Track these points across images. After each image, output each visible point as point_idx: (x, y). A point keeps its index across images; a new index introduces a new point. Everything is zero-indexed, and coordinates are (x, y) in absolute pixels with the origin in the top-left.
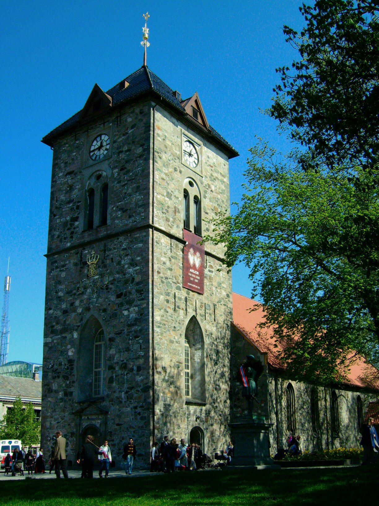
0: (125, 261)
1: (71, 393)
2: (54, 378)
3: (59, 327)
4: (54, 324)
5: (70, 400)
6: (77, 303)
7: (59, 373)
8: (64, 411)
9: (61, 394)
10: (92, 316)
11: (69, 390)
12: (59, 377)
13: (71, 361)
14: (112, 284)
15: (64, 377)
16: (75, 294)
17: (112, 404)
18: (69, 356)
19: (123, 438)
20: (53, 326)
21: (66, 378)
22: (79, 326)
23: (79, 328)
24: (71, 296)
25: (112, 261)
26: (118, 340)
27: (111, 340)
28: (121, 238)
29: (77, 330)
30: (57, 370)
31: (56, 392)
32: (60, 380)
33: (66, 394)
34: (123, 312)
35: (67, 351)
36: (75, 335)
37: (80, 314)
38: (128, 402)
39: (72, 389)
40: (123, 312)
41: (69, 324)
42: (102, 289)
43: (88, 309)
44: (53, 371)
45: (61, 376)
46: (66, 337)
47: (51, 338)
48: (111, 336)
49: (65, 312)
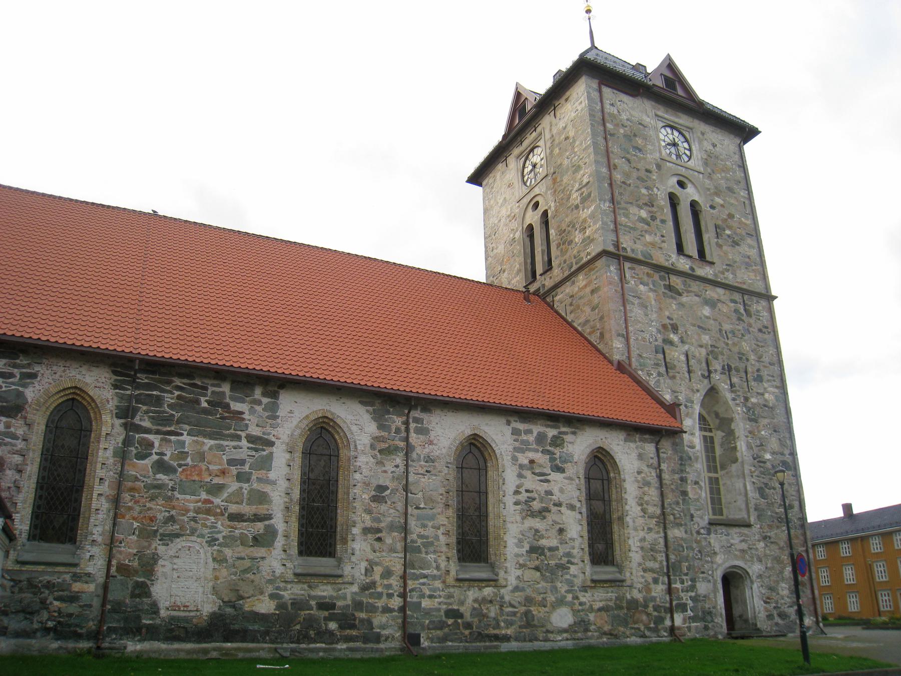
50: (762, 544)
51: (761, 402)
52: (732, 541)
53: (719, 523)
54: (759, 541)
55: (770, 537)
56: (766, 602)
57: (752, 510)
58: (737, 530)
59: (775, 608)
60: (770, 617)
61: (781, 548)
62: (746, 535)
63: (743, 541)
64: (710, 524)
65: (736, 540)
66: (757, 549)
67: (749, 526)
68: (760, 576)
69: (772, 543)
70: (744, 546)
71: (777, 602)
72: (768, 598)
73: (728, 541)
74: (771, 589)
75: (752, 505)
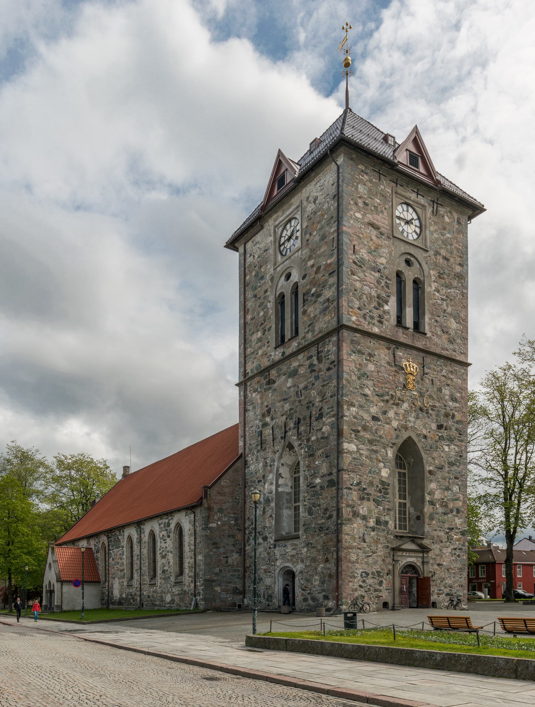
0: (446, 391)
1: (386, 523)
2: (362, 499)
3: (367, 436)
4: (360, 428)
5: (384, 530)
6: (391, 414)
7: (368, 494)
8: (377, 542)
9: (372, 523)
10: (410, 437)
11: (383, 518)
12: (369, 500)
13: (383, 483)
14: (432, 410)
15: (374, 500)
16: (387, 401)
17: (433, 543)
18: (382, 477)
19: (444, 579)
20: (359, 431)
21: (377, 503)
22: (394, 444)
23: (395, 447)
24: (383, 401)
25: (432, 384)
26: (439, 475)
27: (430, 472)
28: (440, 362)
29: (391, 447)
30: (364, 489)
31: (364, 518)
32: (372, 504)
33: (378, 522)
34: (444, 446)
35: (380, 471)
36: (390, 453)
37: (396, 430)
38: (448, 543)
39: (387, 518)
40: (444, 446)
41: (380, 437)
42: (421, 409)
43: (406, 428)
44: (359, 490)
45: (371, 499)
46: (376, 452)
47: (357, 446)
48: (431, 468)
49: (375, 418)
50: (305, 549)
51: (320, 436)
52: (287, 550)
53: (281, 539)
54: (304, 547)
55: (312, 544)
56: (303, 590)
57: (301, 526)
58: (290, 542)
59: (309, 593)
60: (305, 600)
61: (318, 551)
62: (296, 545)
63: (293, 549)
64: (275, 541)
65: (289, 549)
66: (302, 553)
67: (298, 537)
68: (301, 572)
69: (313, 547)
70: (294, 553)
71: (310, 590)
72: (305, 587)
73: (285, 550)
74: (308, 580)
75: (301, 523)
